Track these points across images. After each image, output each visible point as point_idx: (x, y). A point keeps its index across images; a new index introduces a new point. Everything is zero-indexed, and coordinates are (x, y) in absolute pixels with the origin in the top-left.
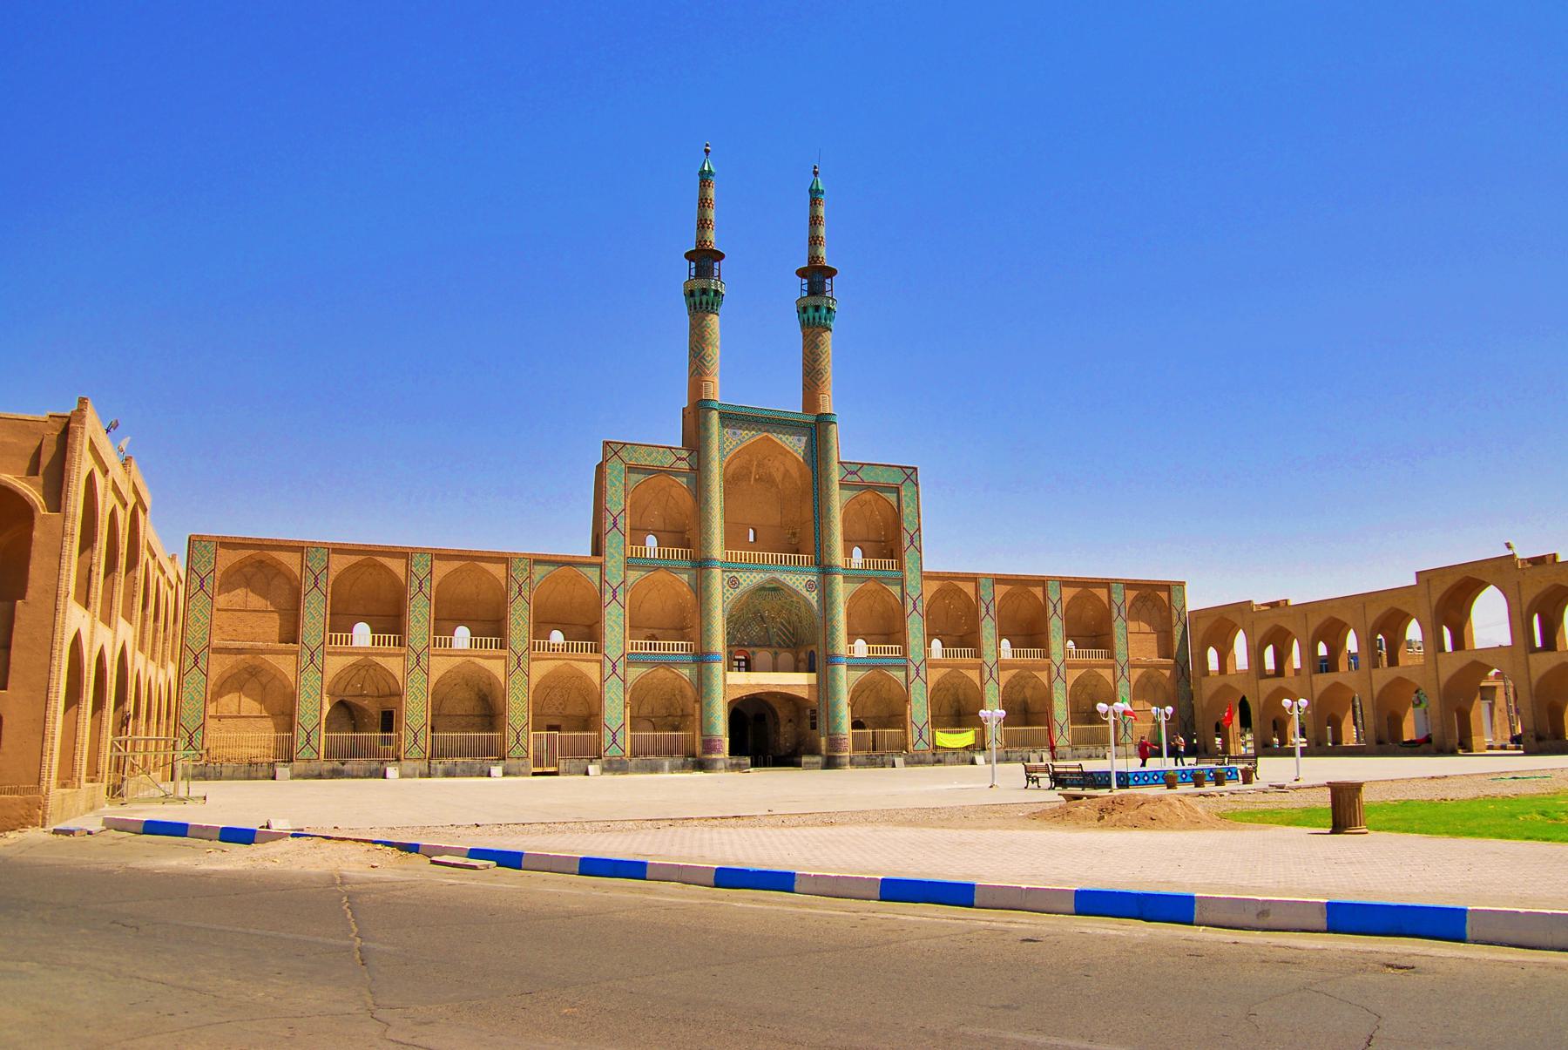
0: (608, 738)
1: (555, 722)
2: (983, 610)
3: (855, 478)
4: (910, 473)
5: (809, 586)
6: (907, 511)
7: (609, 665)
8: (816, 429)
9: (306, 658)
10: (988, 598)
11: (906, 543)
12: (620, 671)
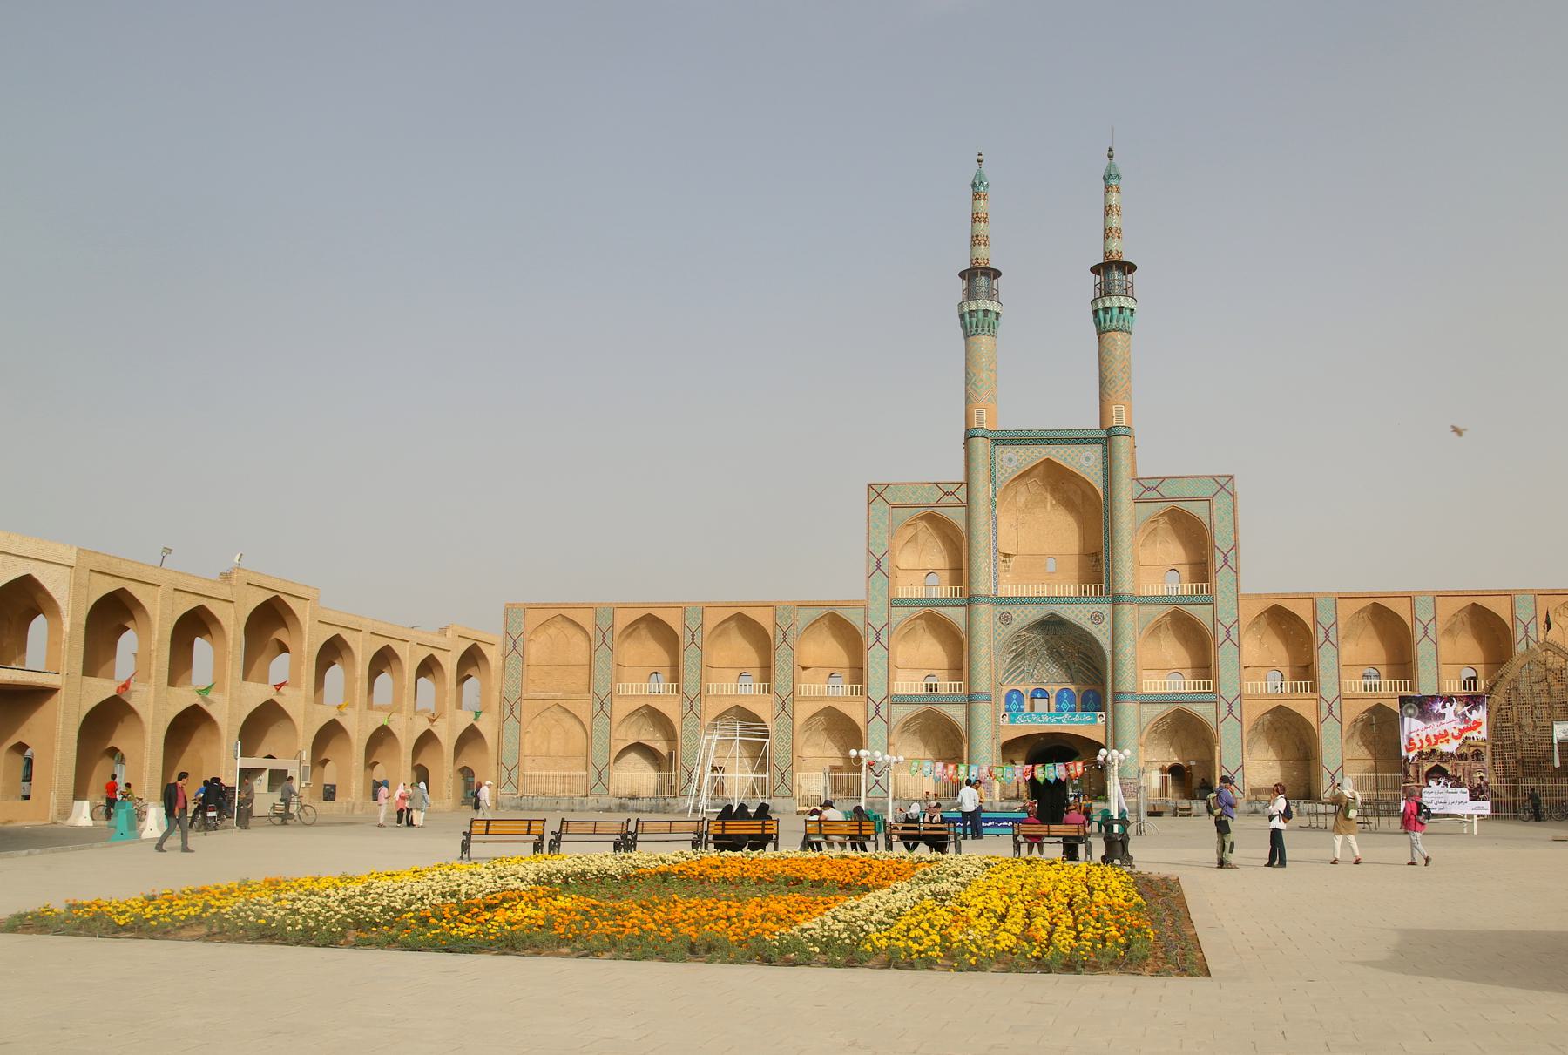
2: (1321, 637)
3: (1154, 495)
4: (1225, 484)
5: (1097, 618)
6: (1218, 527)
7: (872, 707)
9: (597, 706)
11: (1219, 561)
12: (883, 712)
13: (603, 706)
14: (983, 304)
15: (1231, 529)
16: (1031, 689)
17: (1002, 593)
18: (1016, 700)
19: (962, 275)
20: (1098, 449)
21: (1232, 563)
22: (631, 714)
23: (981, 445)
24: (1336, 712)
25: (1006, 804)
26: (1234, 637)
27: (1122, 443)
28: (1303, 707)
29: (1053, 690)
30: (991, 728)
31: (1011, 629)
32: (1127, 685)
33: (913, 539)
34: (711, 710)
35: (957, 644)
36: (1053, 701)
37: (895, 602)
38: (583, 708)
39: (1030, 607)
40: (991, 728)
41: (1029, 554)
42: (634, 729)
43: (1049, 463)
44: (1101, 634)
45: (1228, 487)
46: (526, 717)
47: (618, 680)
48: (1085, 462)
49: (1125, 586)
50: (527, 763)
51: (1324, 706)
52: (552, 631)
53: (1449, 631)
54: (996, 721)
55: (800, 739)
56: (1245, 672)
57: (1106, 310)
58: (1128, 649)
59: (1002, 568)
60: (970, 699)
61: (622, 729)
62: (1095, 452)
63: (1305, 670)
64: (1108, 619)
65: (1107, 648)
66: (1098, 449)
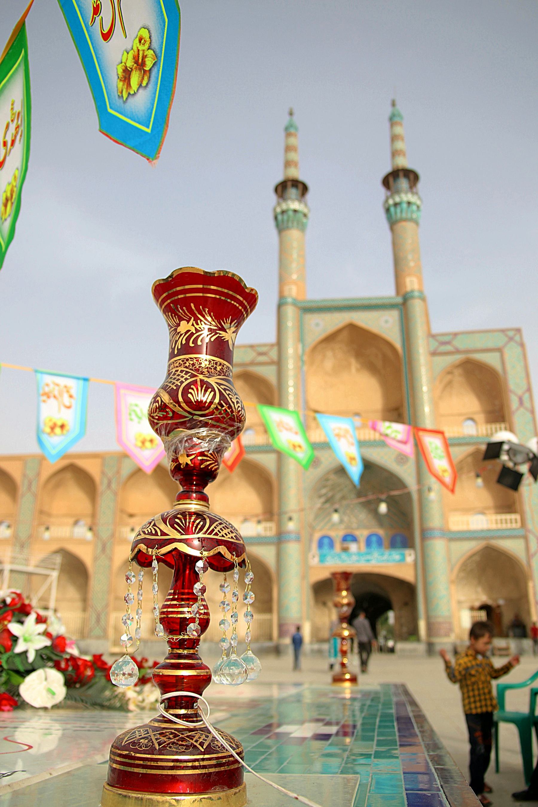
4: (514, 335)
8: (403, 304)
14: (295, 205)
15: (523, 375)
21: (527, 404)
31: (319, 471)
43: (352, 327)
45: (517, 338)
48: (385, 325)
57: (396, 205)
60: (280, 539)
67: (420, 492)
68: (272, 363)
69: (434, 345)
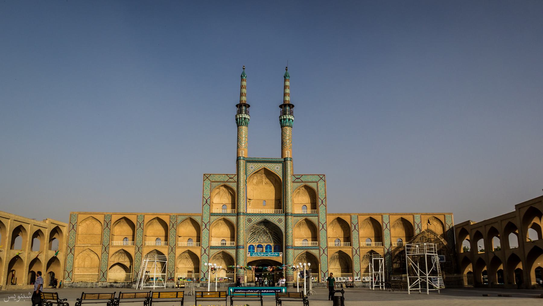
0: (202, 276)
1: (190, 270)
2: (353, 228)
3: (299, 180)
5: (280, 221)
6: (320, 191)
7: (203, 250)
8: (284, 162)
10: (355, 223)
11: (320, 203)
12: (207, 252)
13: (106, 249)
14: (244, 116)
16: (257, 244)
17: (248, 212)
18: (253, 248)
19: (237, 106)
20: (281, 165)
21: (324, 203)
22: (116, 252)
23: (242, 162)
24: (358, 253)
25: (249, 284)
26: (325, 228)
27: (289, 163)
28: (347, 250)
29: (264, 245)
30: (244, 257)
32: (290, 244)
33: (218, 193)
34: (146, 251)
35: (233, 229)
36: (264, 249)
37: (212, 214)
38: (98, 250)
39: (258, 217)
40: (244, 257)
41: (258, 197)
42: (117, 258)
44: (282, 226)
45: (323, 178)
46: (76, 253)
47: (112, 240)
48: (277, 169)
49: (289, 211)
50: (76, 270)
51: (354, 250)
52: (88, 222)
53: (394, 226)
54: (246, 255)
55: (178, 261)
56: (329, 239)
57: (284, 119)
58: (290, 231)
59: (248, 204)
60: (237, 247)
61: (113, 258)
62: (280, 166)
63: (348, 239)
64: (284, 221)
65: (283, 231)
66: (281, 165)
67: (286, 233)
68: (235, 182)
69: (294, 178)
